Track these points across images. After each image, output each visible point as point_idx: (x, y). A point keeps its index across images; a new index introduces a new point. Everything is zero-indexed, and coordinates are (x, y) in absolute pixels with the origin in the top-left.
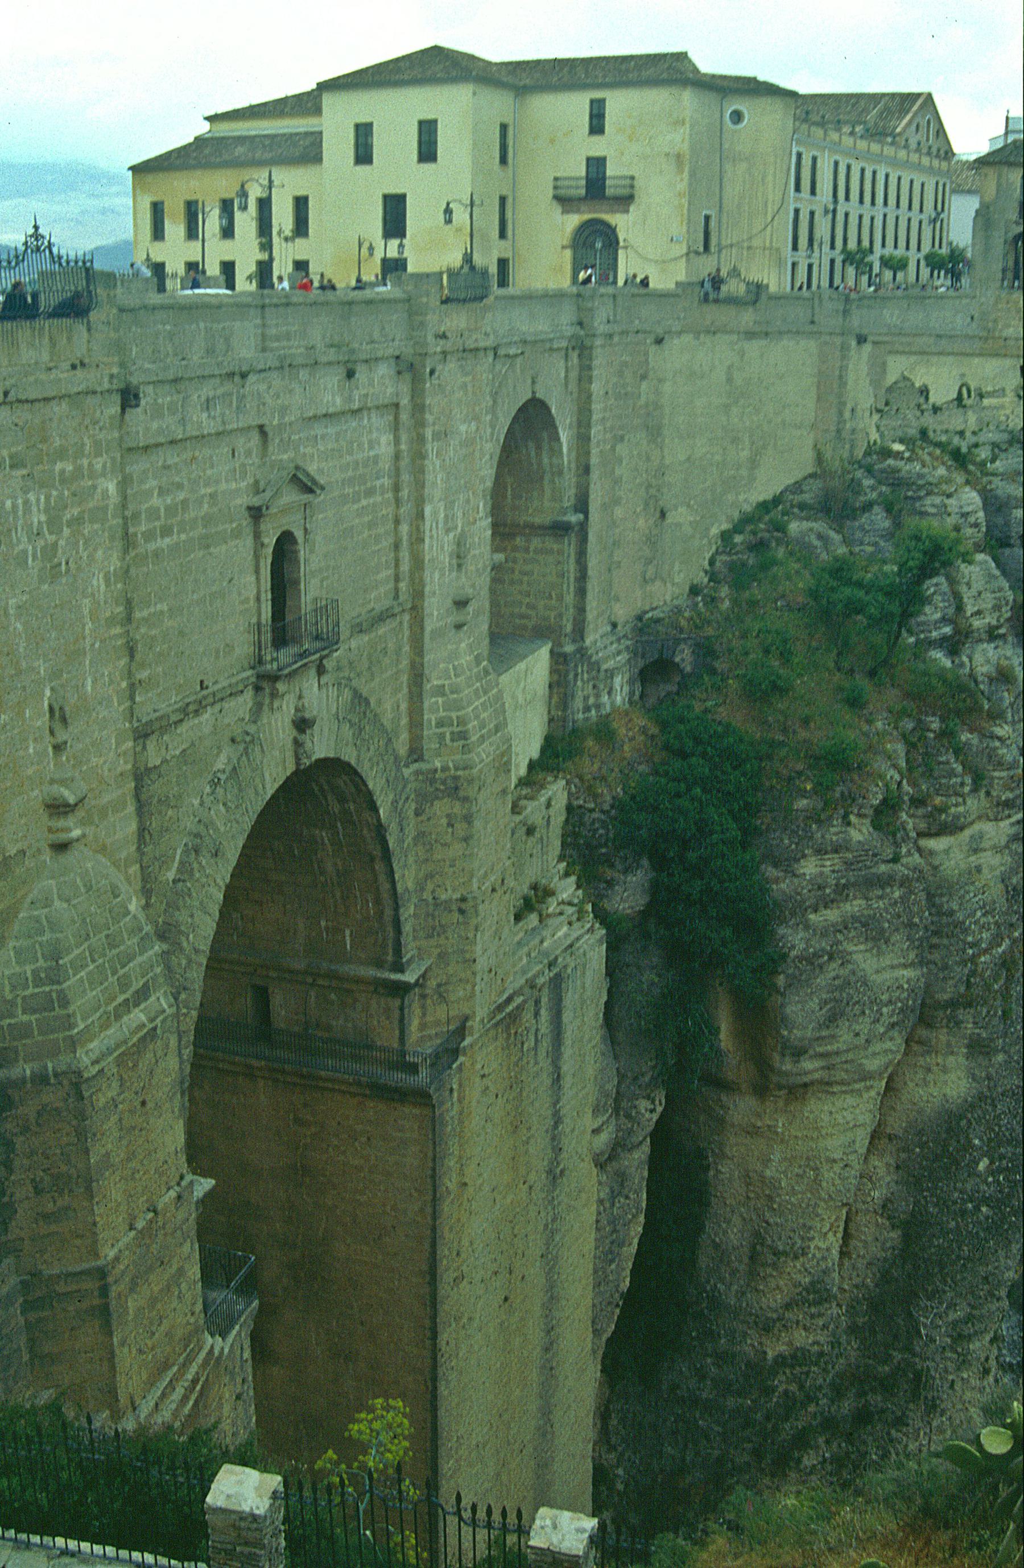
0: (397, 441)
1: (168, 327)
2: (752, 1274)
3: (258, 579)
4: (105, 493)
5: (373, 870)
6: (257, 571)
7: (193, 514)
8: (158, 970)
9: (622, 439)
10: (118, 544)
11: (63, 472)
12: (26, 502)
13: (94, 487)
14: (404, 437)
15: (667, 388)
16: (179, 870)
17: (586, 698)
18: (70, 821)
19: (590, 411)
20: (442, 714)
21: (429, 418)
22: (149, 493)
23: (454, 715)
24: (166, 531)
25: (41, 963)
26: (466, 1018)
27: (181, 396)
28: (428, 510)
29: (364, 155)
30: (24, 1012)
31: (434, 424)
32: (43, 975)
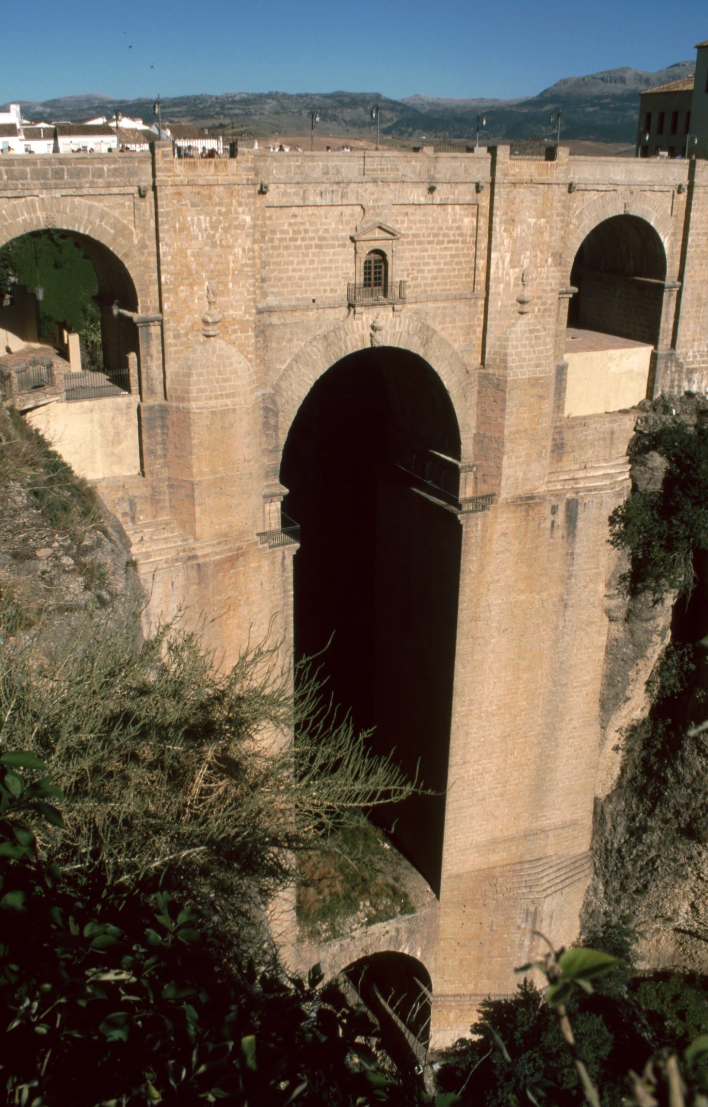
4: (244, 221)
11: (220, 212)
13: (237, 219)
16: (288, 367)
18: (210, 328)
22: (283, 224)
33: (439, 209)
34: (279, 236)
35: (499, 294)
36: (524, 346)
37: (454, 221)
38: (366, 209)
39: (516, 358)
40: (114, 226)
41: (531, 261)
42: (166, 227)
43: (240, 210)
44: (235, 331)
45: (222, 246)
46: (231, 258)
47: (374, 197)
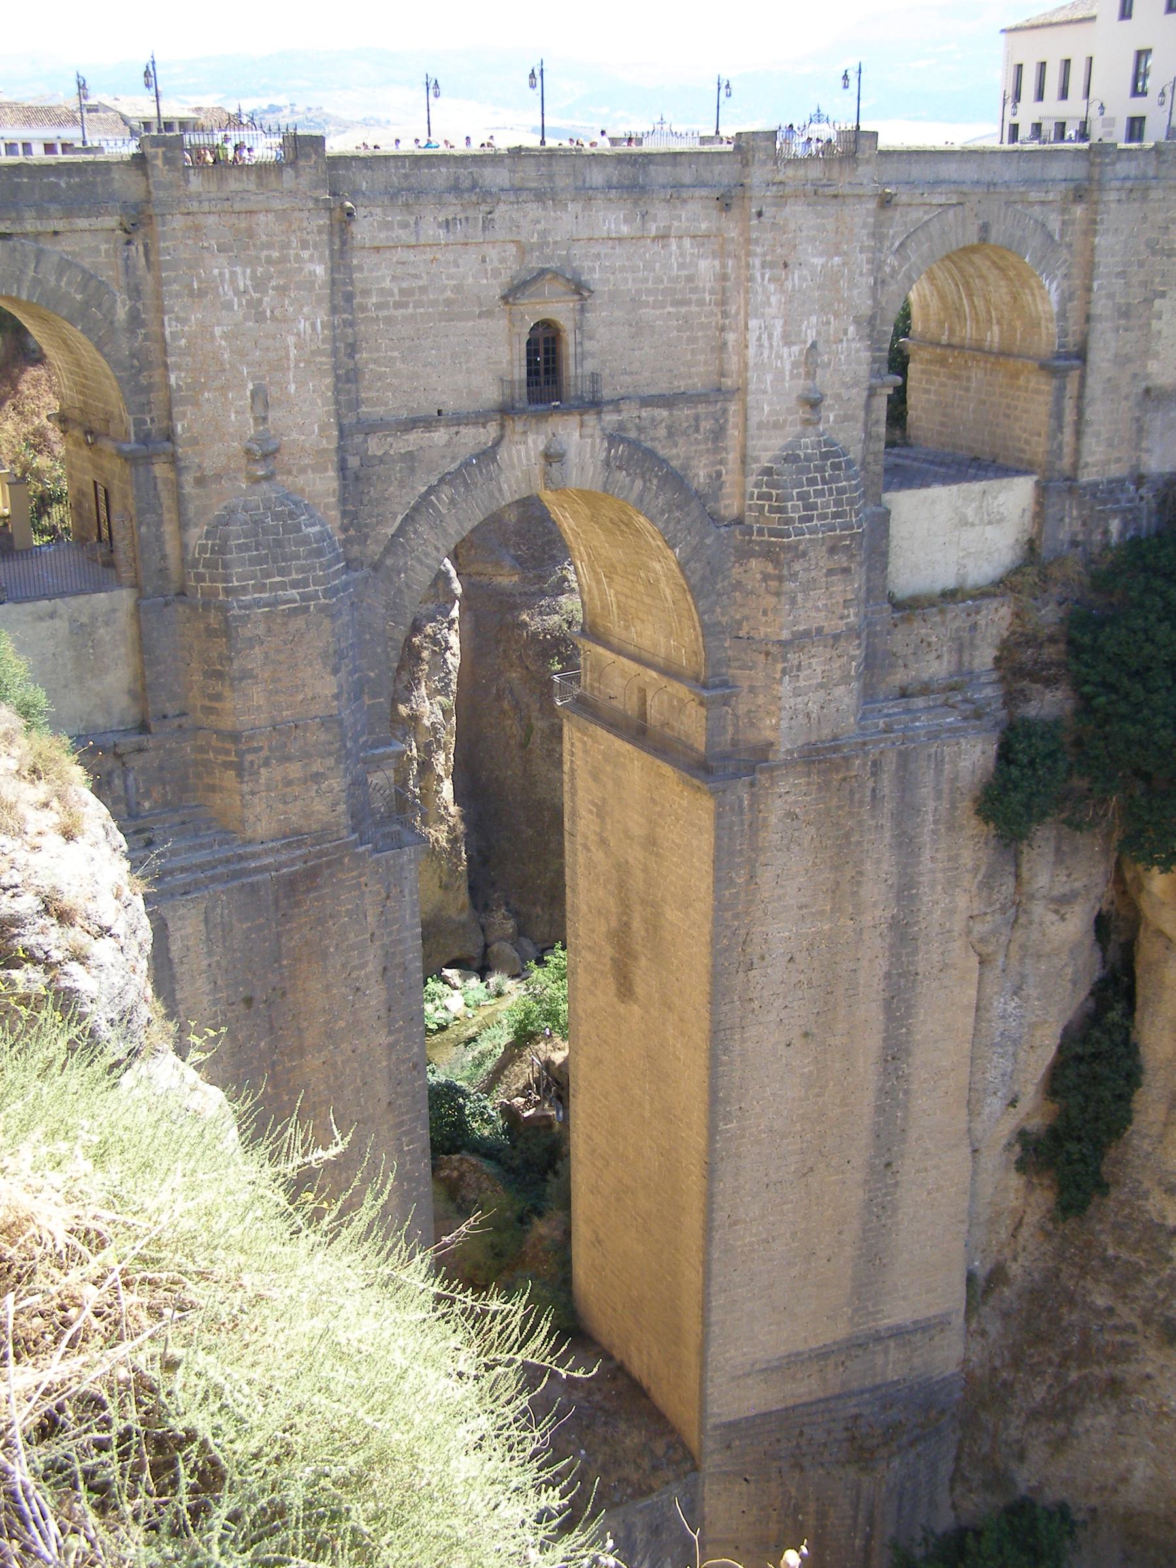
0: (723, 266)
4: (312, 273)
9: (1163, 295)
11: (268, 257)
12: (233, 273)
13: (301, 269)
19: (1093, 262)
20: (765, 489)
22: (383, 278)
23: (774, 492)
24: (398, 305)
28: (753, 323)
33: (657, 247)
34: (374, 300)
35: (765, 392)
36: (812, 482)
37: (682, 266)
40: (83, 287)
41: (818, 333)
42: (176, 287)
43: (305, 254)
44: (303, 470)
45: (274, 318)
46: (291, 340)
47: (538, 227)
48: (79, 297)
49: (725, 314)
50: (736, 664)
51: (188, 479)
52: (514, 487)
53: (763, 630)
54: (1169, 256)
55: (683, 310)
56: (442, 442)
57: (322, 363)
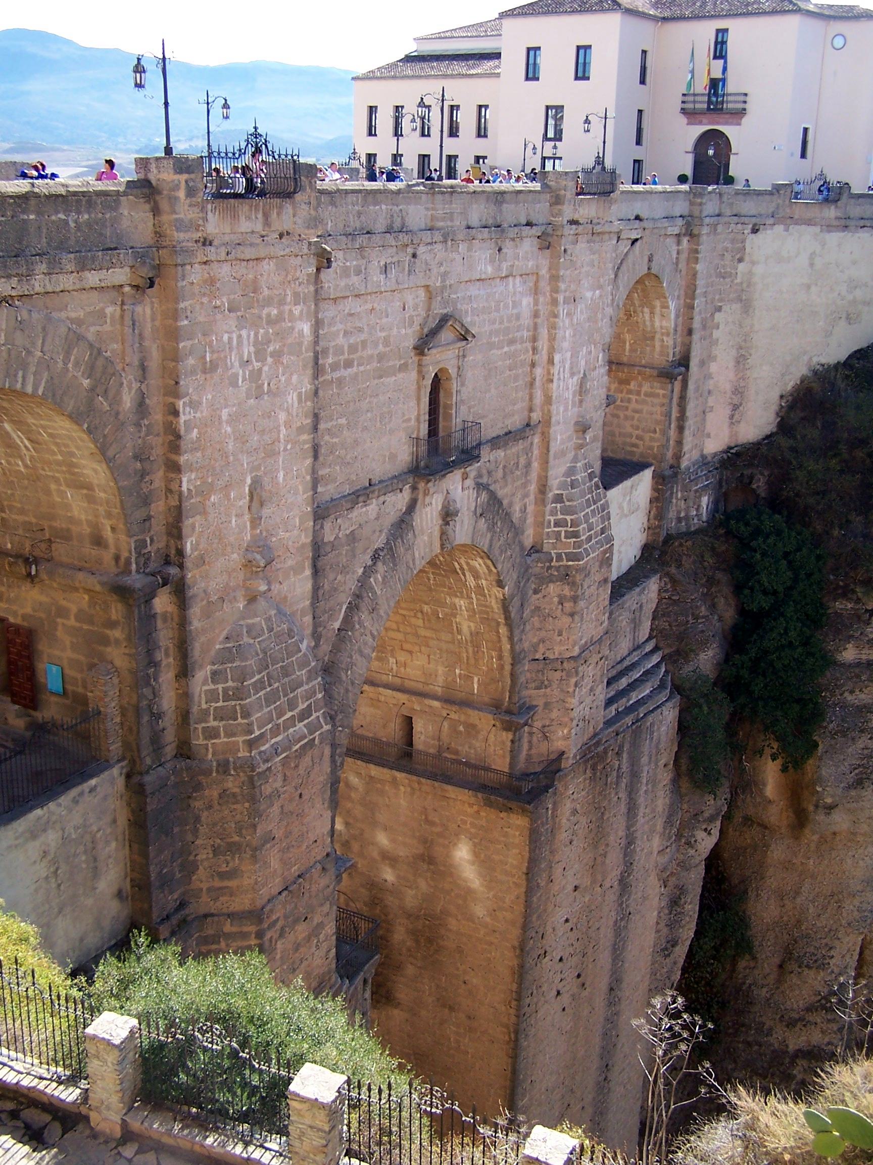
0: (536, 303)
1: (356, 208)
2: (779, 981)
3: (418, 405)
5: (498, 632)
6: (419, 399)
7: (370, 352)
8: (320, 696)
9: (719, 309)
10: (309, 372)
11: (269, 315)
13: (293, 328)
14: (541, 299)
15: (759, 270)
17: (679, 512)
19: (695, 285)
20: (560, 517)
21: (562, 286)
23: (568, 518)
24: (348, 364)
25: (230, 684)
26: (563, 753)
27: (364, 261)
28: (557, 358)
29: (532, 74)
30: (215, 720)
31: (566, 291)
32: (231, 693)
38: (434, 293)
39: (585, 525)
42: (191, 361)
43: (297, 310)
46: (282, 416)
47: (442, 269)
48: (86, 383)
49: (535, 350)
50: (533, 685)
51: (195, 612)
52: (422, 554)
53: (557, 649)
54: (724, 278)
55: (513, 348)
56: (373, 516)
57: (305, 442)
